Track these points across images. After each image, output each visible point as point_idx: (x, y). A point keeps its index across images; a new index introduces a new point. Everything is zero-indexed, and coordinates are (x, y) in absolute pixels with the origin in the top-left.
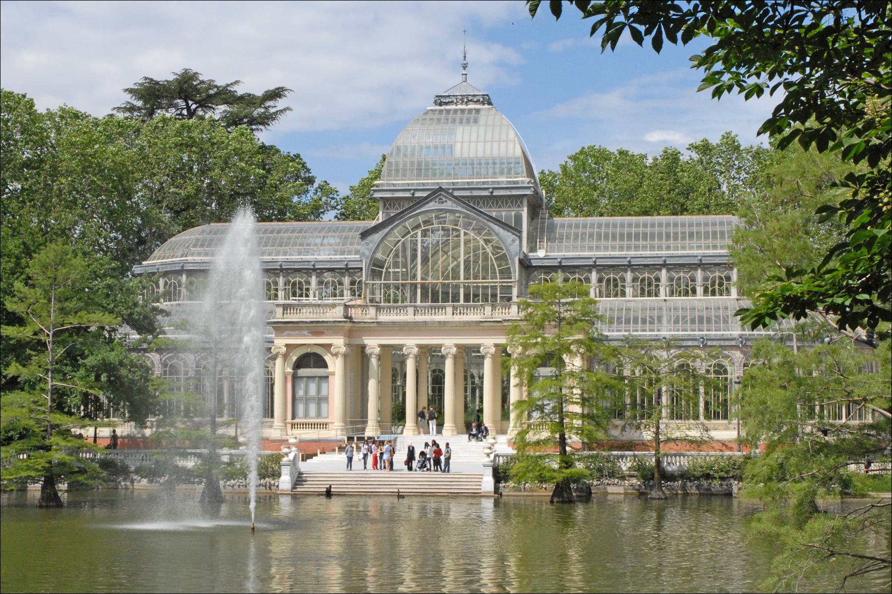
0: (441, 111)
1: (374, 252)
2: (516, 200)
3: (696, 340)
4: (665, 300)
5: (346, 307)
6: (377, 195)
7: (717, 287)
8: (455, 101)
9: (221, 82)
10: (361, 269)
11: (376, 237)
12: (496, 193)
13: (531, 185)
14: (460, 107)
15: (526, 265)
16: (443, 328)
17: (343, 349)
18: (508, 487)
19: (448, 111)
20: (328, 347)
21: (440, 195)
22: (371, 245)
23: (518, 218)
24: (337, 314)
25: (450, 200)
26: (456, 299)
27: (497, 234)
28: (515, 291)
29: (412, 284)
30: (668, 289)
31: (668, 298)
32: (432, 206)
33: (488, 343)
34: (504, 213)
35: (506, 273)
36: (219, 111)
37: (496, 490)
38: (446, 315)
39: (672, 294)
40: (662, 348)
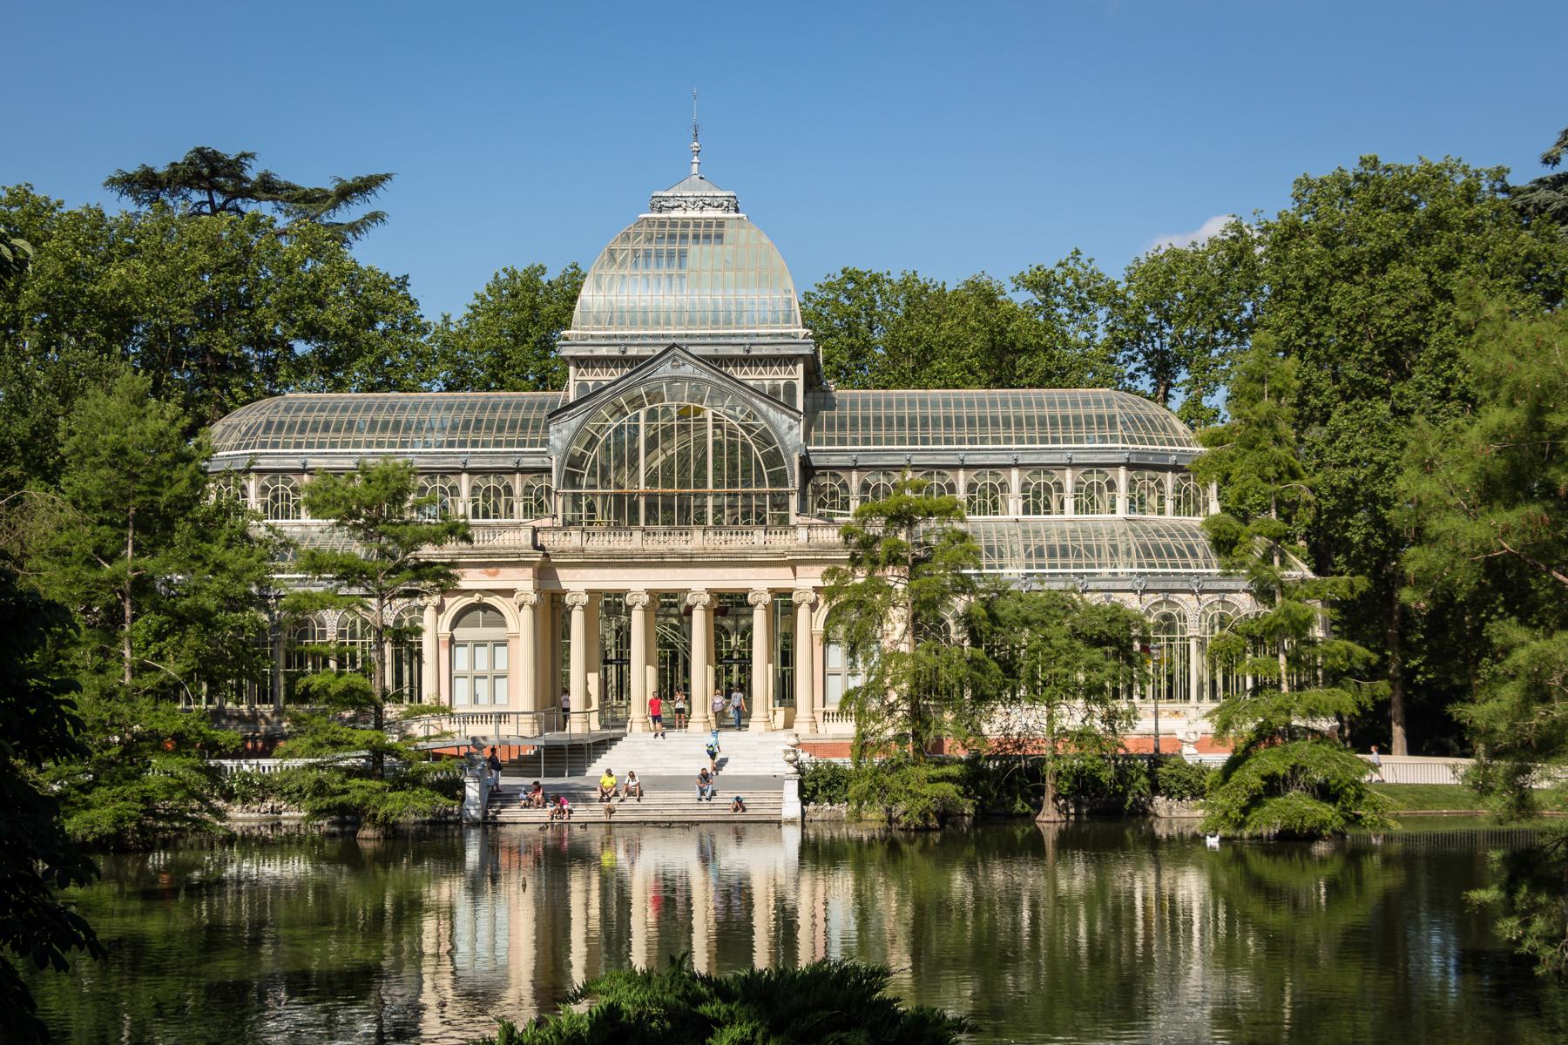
1: (570, 444)
2: (791, 360)
4: (1017, 520)
6: (567, 352)
7: (989, 502)
8: (684, 205)
10: (549, 470)
12: (755, 352)
14: (691, 214)
16: (688, 561)
17: (533, 598)
20: (509, 593)
22: (565, 432)
23: (790, 388)
25: (690, 362)
26: (701, 519)
27: (766, 417)
28: (794, 502)
31: (1021, 517)
34: (767, 383)
35: (779, 479)
37: (803, 814)
38: (697, 541)
40: (1193, 592)
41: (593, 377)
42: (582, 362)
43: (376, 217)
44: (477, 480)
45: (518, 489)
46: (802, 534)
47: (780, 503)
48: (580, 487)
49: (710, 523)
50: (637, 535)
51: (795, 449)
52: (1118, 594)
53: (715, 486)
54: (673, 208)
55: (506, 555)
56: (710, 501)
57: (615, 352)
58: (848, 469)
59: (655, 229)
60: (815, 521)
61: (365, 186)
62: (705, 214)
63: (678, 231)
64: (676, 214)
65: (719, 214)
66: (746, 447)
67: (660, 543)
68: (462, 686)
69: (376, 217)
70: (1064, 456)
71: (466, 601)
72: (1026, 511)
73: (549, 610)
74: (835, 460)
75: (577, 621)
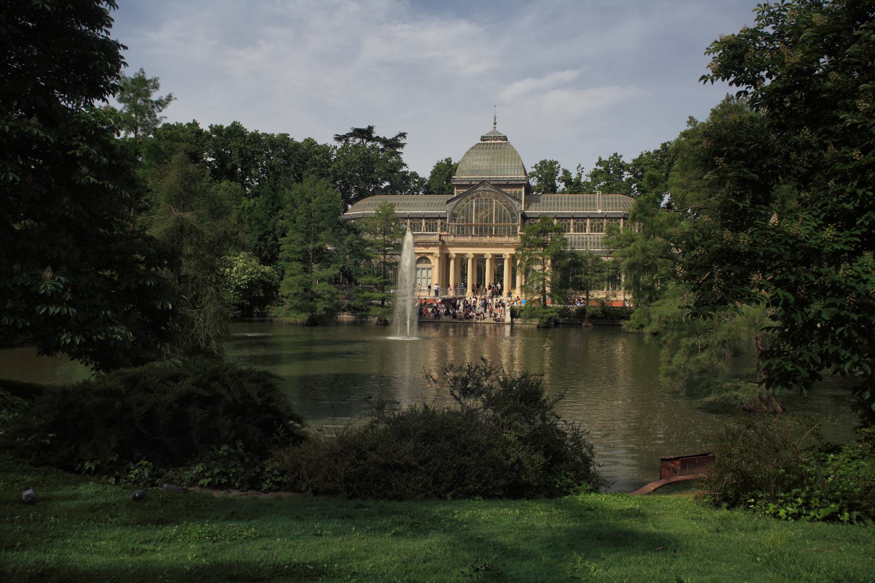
0: (484, 144)
5: (440, 236)
6: (454, 183)
11: (455, 202)
15: (524, 218)
16: (485, 245)
17: (438, 255)
18: (518, 321)
19: (487, 144)
20: (431, 254)
23: (520, 193)
24: (436, 238)
28: (519, 228)
32: (480, 188)
33: (507, 252)
38: (487, 239)
41: (461, 191)
42: (459, 186)
44: (427, 221)
56: (494, 228)
57: (468, 183)
65: (501, 142)
66: (505, 210)
67: (476, 240)
74: (533, 216)
75: (452, 263)
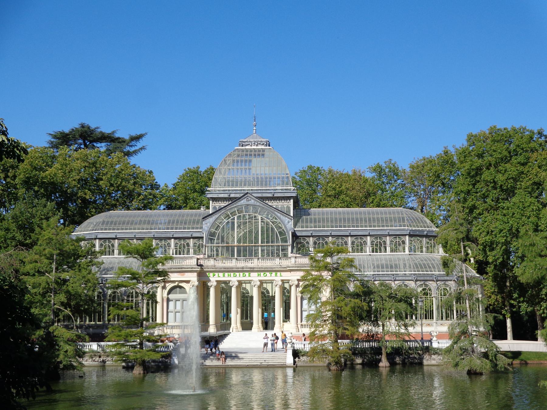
1: (210, 228)
2: (289, 198)
3: (369, 277)
4: (370, 255)
6: (209, 196)
9: (106, 130)
10: (202, 238)
12: (276, 195)
13: (295, 191)
14: (253, 147)
16: (252, 270)
17: (196, 283)
20: (188, 282)
21: (247, 196)
22: (208, 224)
23: (289, 208)
25: (253, 199)
26: (256, 254)
27: (280, 218)
28: (290, 248)
29: (227, 247)
30: (371, 248)
31: (371, 253)
32: (243, 202)
36: (102, 147)
38: (255, 263)
39: (373, 252)
40: (434, 281)
42: (214, 199)
43: (143, 148)
45: (191, 245)
46: (293, 260)
47: (284, 249)
48: (214, 243)
49: (260, 256)
50: (234, 261)
51: (290, 230)
52: (407, 282)
53: (262, 243)
54: (247, 145)
55: (188, 268)
57: (226, 196)
58: (114, 239)
59: (240, 153)
60: (297, 255)
61: (138, 138)
62: (258, 147)
63: (249, 153)
64: (247, 147)
65: (263, 147)
66: (272, 229)
67: (241, 264)
68: (171, 315)
69: (141, 149)
70: (329, 233)
71: (173, 285)
72: (373, 252)
73: (202, 288)
74: (304, 234)
